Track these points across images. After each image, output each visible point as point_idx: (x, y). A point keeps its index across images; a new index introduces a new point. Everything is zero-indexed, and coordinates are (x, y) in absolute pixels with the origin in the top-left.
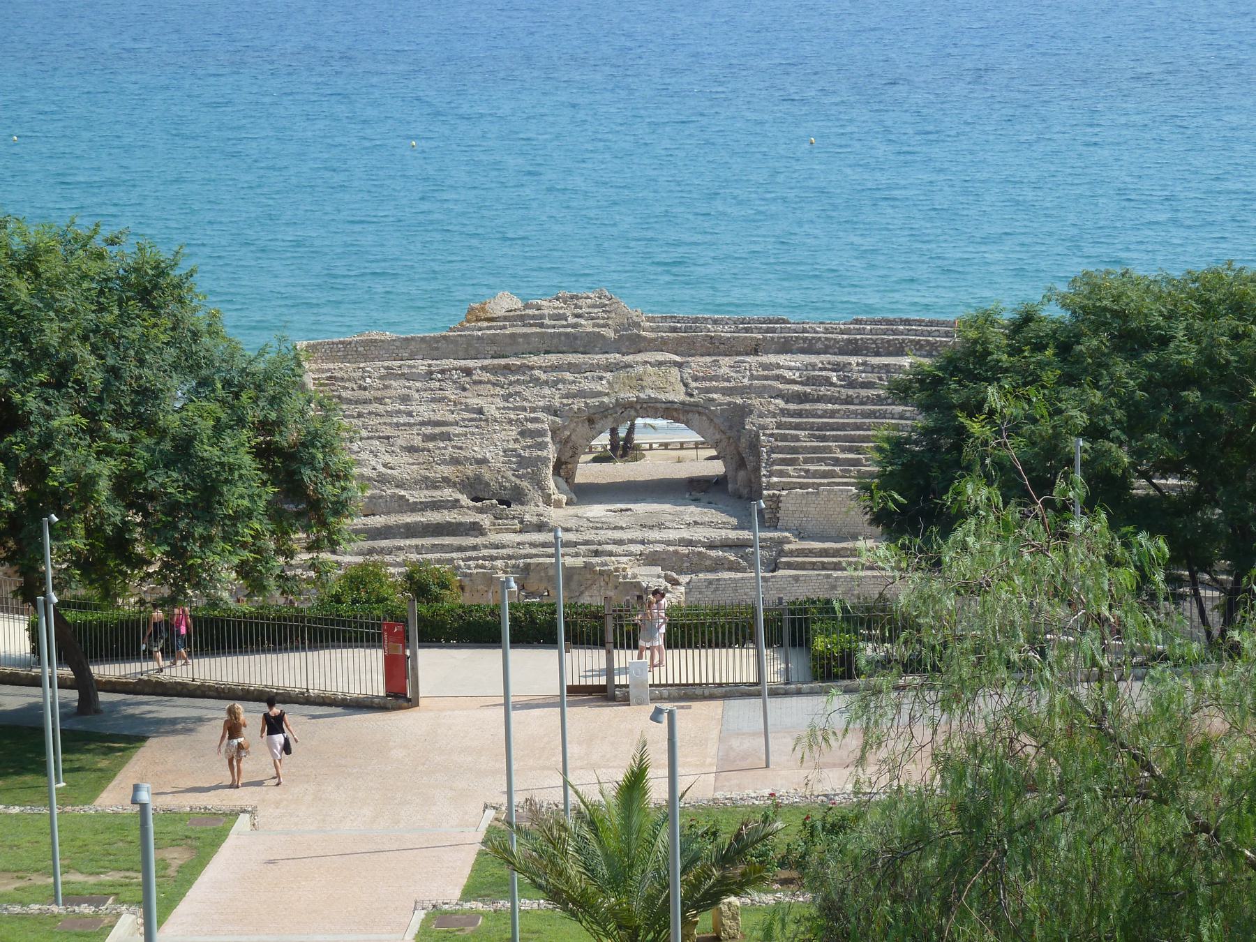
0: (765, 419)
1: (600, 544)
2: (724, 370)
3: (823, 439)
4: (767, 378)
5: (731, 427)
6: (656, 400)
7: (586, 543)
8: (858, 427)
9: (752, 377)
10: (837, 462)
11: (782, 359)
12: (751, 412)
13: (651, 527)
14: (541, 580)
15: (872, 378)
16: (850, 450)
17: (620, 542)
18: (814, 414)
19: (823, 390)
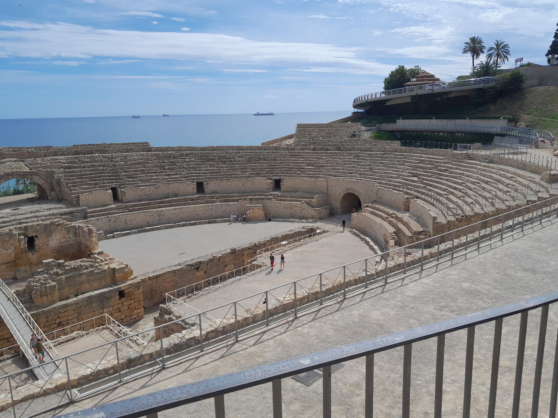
0: (59, 174)
1: (19, 220)
2: (39, 161)
3: (82, 178)
4: (55, 163)
5: (48, 179)
6: (20, 172)
7: (14, 220)
8: (91, 174)
9: (50, 163)
10: (90, 184)
11: (57, 157)
12: (55, 173)
13: (35, 212)
14: (34, 232)
15: (89, 160)
16: (92, 181)
17: (27, 218)
18: (75, 172)
19: (76, 165)
